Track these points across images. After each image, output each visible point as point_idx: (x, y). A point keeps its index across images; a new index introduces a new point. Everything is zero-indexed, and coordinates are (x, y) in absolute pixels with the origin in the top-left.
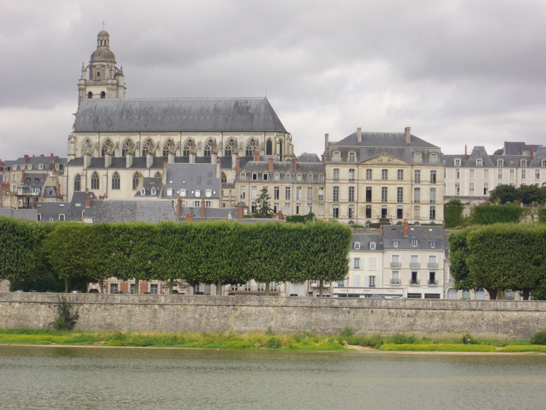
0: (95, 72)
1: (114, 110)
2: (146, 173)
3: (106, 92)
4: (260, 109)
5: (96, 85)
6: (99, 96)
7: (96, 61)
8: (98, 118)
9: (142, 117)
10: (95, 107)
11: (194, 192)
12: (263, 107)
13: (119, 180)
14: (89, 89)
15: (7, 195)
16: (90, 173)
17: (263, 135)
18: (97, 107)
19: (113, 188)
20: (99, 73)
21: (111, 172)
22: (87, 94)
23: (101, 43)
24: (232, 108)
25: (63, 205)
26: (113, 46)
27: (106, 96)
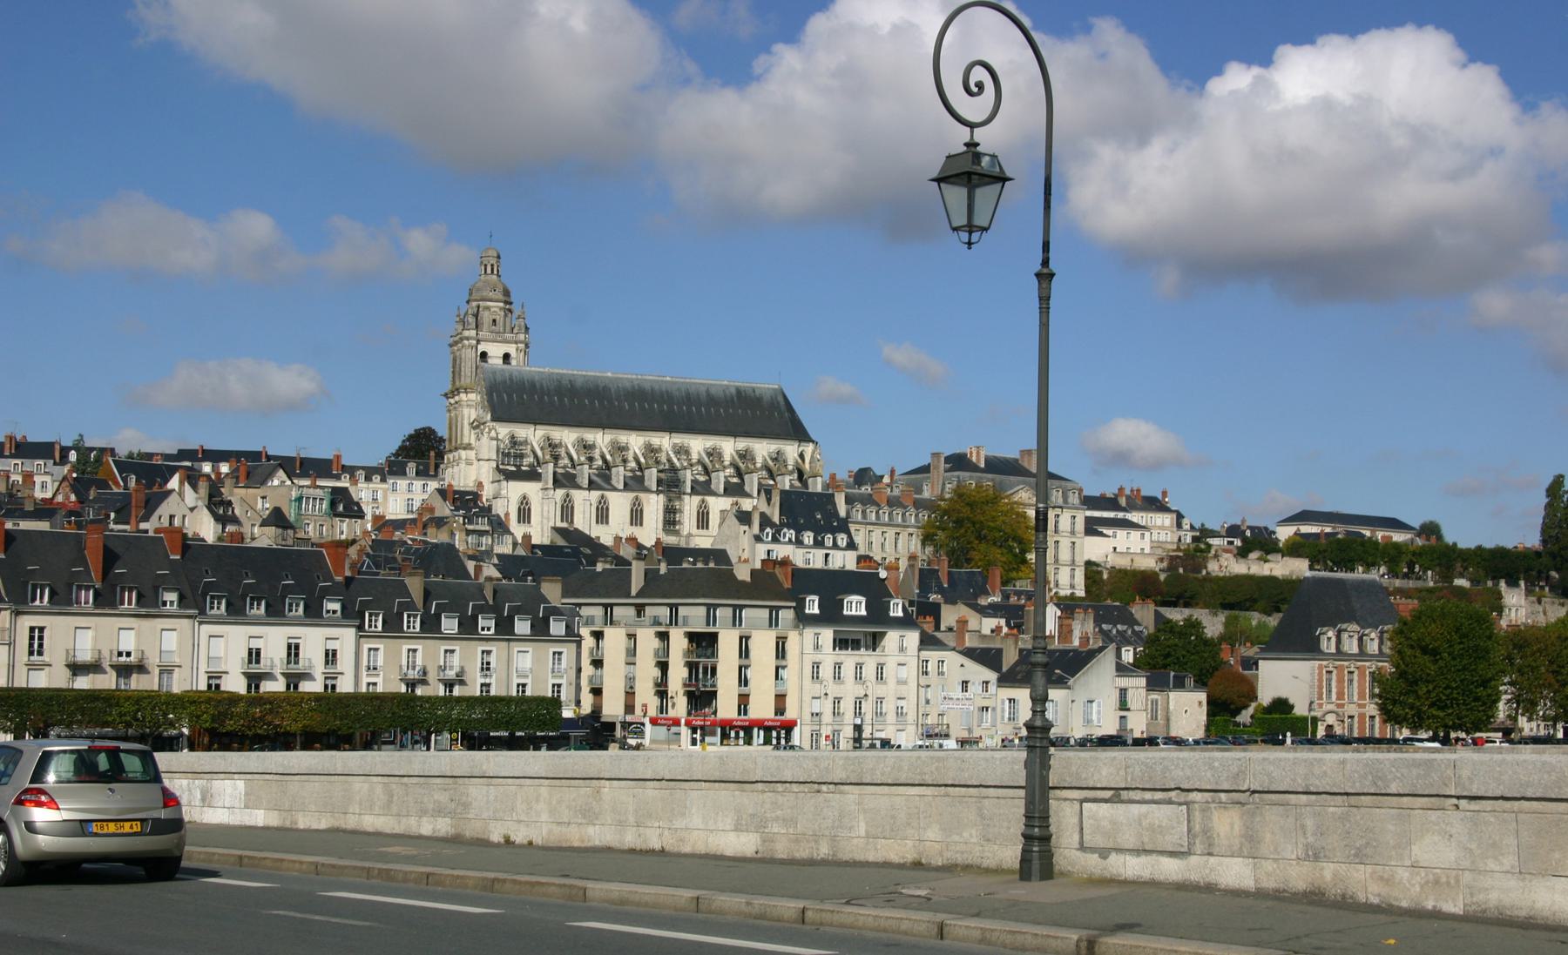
1: (546, 389)
4: (778, 403)
6: (501, 361)
7: (491, 301)
10: (511, 379)
11: (823, 538)
12: (780, 399)
13: (607, 509)
14: (481, 348)
16: (560, 493)
18: (514, 378)
19: (597, 522)
20: (494, 321)
21: (595, 495)
22: (479, 354)
23: (492, 270)
24: (735, 398)
25: (569, 550)
27: (514, 362)
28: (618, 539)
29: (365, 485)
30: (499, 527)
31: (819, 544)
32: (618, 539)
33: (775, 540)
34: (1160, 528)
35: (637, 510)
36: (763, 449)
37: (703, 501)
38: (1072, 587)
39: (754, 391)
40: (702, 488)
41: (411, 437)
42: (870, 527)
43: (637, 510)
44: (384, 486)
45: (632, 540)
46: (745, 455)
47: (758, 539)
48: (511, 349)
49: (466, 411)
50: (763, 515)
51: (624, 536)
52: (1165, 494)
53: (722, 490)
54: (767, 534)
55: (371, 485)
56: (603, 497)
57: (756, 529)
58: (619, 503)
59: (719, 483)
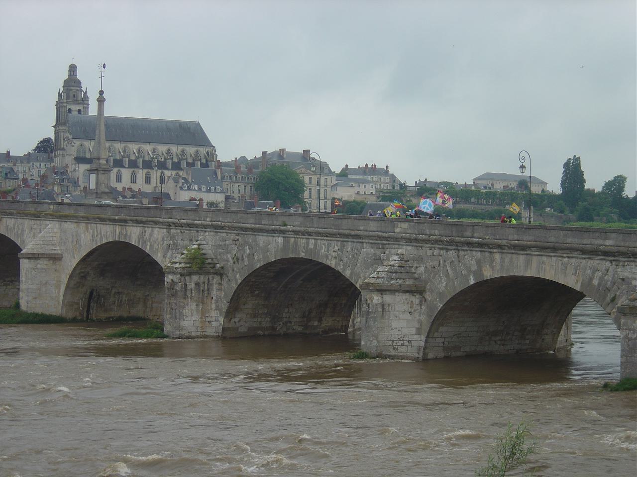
0: (71, 94)
2: (167, 173)
3: (82, 110)
5: (74, 104)
7: (73, 86)
8: (86, 129)
9: (118, 131)
10: (81, 121)
11: (210, 188)
14: (69, 107)
15: (55, 184)
17: (205, 148)
20: (74, 96)
23: (74, 73)
26: (80, 76)
27: (82, 113)
28: (124, 188)
29: (20, 165)
30: (76, 183)
31: (209, 191)
32: (124, 188)
33: (189, 189)
34: (384, 183)
35: (134, 176)
36: (191, 150)
37: (162, 173)
38: (325, 208)
39: (187, 124)
40: (162, 166)
41: (41, 142)
42: (232, 184)
43: (134, 176)
44: (29, 165)
45: (130, 189)
46: (183, 151)
47: (181, 188)
48: (81, 107)
49: (62, 134)
50: (184, 179)
51: (127, 187)
52: (387, 167)
53: (170, 168)
54: (185, 186)
55: (23, 165)
56: (119, 170)
57: (180, 184)
58: (126, 173)
59: (169, 165)
